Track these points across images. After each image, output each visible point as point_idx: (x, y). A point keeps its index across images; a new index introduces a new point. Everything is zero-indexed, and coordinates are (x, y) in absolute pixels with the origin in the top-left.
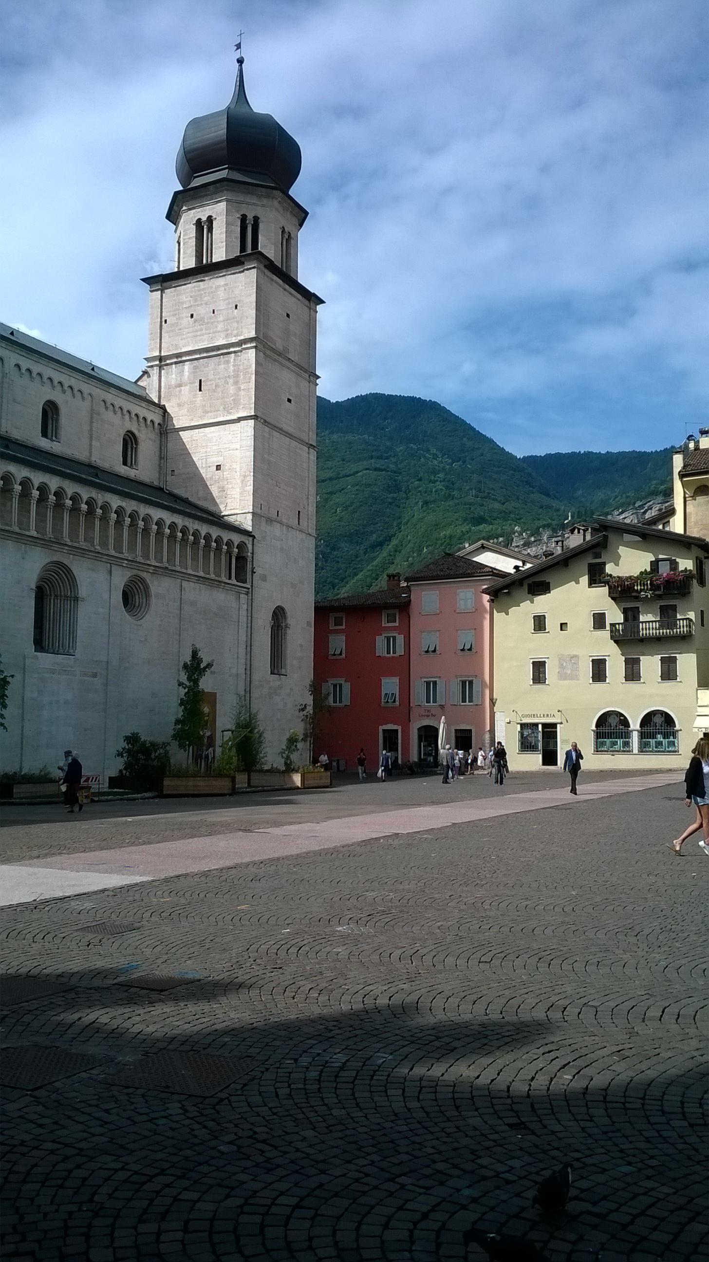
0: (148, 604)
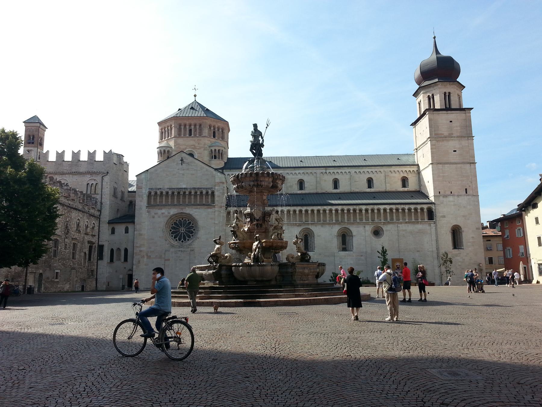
0: (384, 233)
